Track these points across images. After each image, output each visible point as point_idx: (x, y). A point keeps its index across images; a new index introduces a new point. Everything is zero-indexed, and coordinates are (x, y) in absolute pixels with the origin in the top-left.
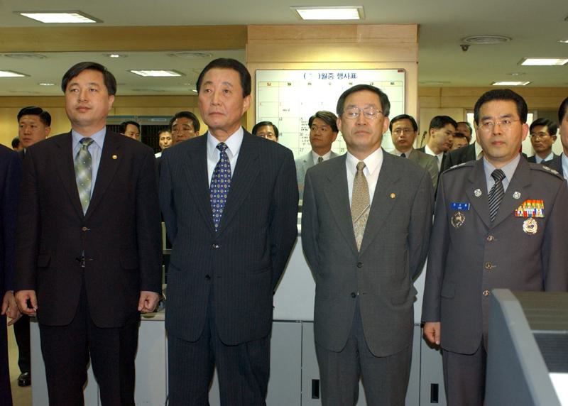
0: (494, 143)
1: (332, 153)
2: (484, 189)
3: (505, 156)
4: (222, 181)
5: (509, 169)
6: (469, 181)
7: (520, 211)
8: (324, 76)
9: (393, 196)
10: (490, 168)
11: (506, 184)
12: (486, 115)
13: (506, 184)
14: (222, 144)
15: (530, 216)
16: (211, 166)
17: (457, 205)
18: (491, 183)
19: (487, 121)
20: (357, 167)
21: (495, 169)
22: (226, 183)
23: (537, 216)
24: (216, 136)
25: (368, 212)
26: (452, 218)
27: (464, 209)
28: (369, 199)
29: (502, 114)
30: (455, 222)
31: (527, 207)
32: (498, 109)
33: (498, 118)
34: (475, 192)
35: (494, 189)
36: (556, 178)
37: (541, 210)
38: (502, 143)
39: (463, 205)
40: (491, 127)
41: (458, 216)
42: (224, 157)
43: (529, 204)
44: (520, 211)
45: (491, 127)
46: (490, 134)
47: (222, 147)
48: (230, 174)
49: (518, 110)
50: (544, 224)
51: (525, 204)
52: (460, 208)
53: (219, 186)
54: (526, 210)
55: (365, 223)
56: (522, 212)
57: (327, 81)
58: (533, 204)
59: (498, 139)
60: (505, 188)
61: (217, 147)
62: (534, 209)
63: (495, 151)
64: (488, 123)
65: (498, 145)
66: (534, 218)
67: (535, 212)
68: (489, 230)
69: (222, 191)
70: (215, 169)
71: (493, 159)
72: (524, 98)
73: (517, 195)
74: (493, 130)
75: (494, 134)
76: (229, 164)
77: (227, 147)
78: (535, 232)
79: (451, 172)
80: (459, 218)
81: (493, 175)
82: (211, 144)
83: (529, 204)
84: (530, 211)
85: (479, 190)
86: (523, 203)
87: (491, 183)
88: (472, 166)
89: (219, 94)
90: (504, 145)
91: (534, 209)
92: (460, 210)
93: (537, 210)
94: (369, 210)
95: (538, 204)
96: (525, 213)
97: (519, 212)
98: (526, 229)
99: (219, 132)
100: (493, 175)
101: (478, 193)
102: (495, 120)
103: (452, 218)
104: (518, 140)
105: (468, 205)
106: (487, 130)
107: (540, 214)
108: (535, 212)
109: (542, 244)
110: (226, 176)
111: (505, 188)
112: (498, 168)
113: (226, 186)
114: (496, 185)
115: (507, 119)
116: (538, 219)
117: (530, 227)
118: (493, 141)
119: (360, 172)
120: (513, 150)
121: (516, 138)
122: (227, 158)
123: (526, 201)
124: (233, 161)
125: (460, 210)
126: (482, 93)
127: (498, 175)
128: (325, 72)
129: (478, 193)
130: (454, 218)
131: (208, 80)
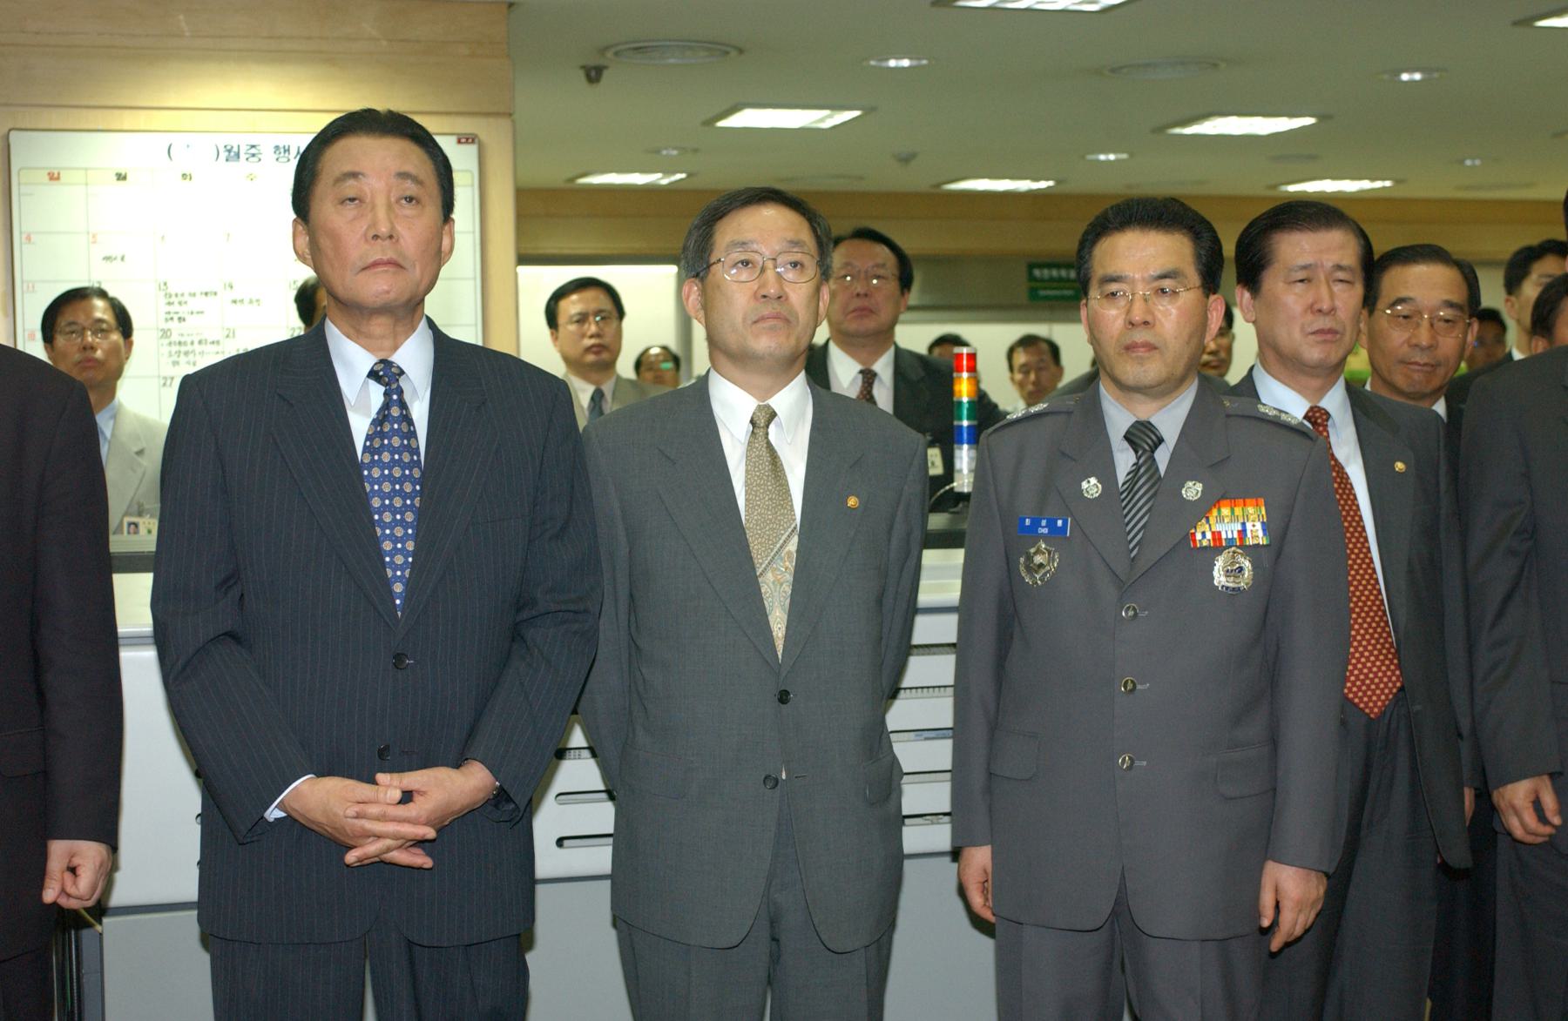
0: (1130, 348)
1: (619, 378)
2: (1106, 472)
3: (1159, 385)
4: (397, 472)
5: (1170, 419)
6: (1063, 454)
7: (1203, 534)
8: (233, 155)
9: (852, 502)
10: (1118, 417)
11: (1162, 457)
12: (1112, 270)
13: (1162, 457)
14: (386, 363)
15: (1230, 541)
16: (360, 426)
17: (1036, 523)
19: (1114, 287)
20: (752, 422)
21: (1134, 420)
22: (410, 478)
23: (1250, 541)
24: (357, 335)
25: (793, 546)
26: (1022, 560)
28: (792, 509)
29: (1158, 273)
30: (1032, 569)
31: (1221, 519)
32: (1139, 254)
33: (1143, 279)
34: (1190, 484)
35: (1135, 473)
36: (1297, 438)
37: (1259, 526)
38: (1151, 347)
39: (1051, 524)
40: (1122, 303)
41: (1038, 552)
42: (395, 400)
43: (1226, 511)
44: (1203, 534)
45: (1122, 303)
46: (1119, 323)
47: (386, 374)
48: (417, 451)
49: (1198, 257)
50: (1270, 559)
51: (1215, 512)
52: (1045, 531)
53: (387, 487)
55: (789, 577)
56: (1209, 535)
57: (242, 166)
58: (1238, 511)
59: (1140, 336)
60: (1162, 468)
61: (373, 374)
62: (1241, 523)
63: (1131, 371)
64: (1113, 294)
65: (1141, 352)
66: (1242, 546)
67: (1242, 533)
68: (1125, 589)
69: (398, 502)
70: (369, 437)
71: (1124, 388)
72: (1216, 226)
74: (1128, 312)
75: (1131, 324)
76: (410, 422)
77: (402, 372)
79: (1006, 431)
80: (1038, 559)
81: (1128, 437)
82: (348, 364)
83: (1226, 511)
84: (1229, 530)
85: (1093, 480)
86: (1210, 511)
88: (1069, 413)
89: (389, 207)
90: (1156, 354)
91: (1241, 523)
93: (1249, 526)
94: (795, 539)
95: (1251, 510)
96: (1217, 536)
97: (1199, 536)
99: (379, 325)
100: (1128, 437)
101: (1091, 487)
102: (1133, 282)
103: (1022, 560)
104: (1195, 341)
105: (1065, 523)
106: (1113, 312)
108: (1242, 533)
109: (1266, 613)
110: (406, 458)
111: (1162, 468)
112: (1143, 417)
113: (408, 488)
114: (1137, 466)
115: (1167, 284)
116: (1252, 551)
118: (1128, 342)
119: (760, 432)
120: (1180, 370)
121: (1190, 337)
122: (403, 405)
123: (1217, 503)
124: (420, 411)
125: (1043, 536)
126: (1095, 212)
127: (1143, 437)
128: (233, 141)
129: (1091, 487)
130: (1029, 558)
131: (348, 168)
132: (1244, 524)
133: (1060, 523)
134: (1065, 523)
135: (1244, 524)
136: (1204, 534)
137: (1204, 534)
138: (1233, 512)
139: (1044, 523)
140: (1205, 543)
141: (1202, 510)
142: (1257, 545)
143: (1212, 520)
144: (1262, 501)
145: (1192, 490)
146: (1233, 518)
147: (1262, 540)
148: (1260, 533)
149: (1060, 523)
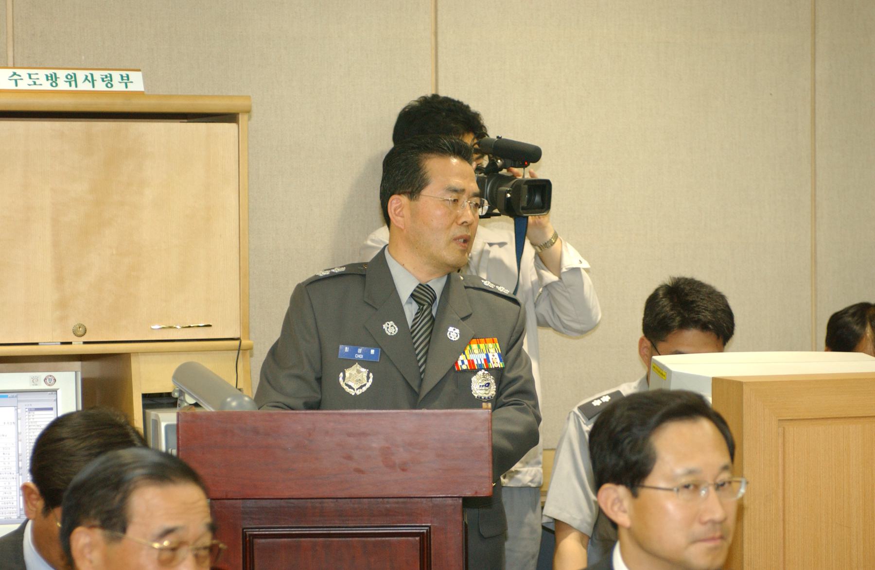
2: (400, 319)
7: (463, 362)
15: (481, 365)
37: (497, 356)
43: (474, 346)
52: (361, 357)
58: (482, 346)
66: (488, 369)
67: (487, 360)
86: (465, 348)
92: (363, 363)
93: (490, 355)
95: (490, 345)
96: (471, 362)
97: (460, 363)
101: (391, 328)
107: (496, 362)
108: (487, 360)
129: (391, 328)
132: (487, 355)
135: (487, 355)
136: (463, 362)
137: (463, 362)
138: (479, 347)
140: (464, 367)
141: (460, 347)
142: (497, 369)
144: (495, 339)
146: (481, 351)
147: (500, 365)
148: (498, 360)
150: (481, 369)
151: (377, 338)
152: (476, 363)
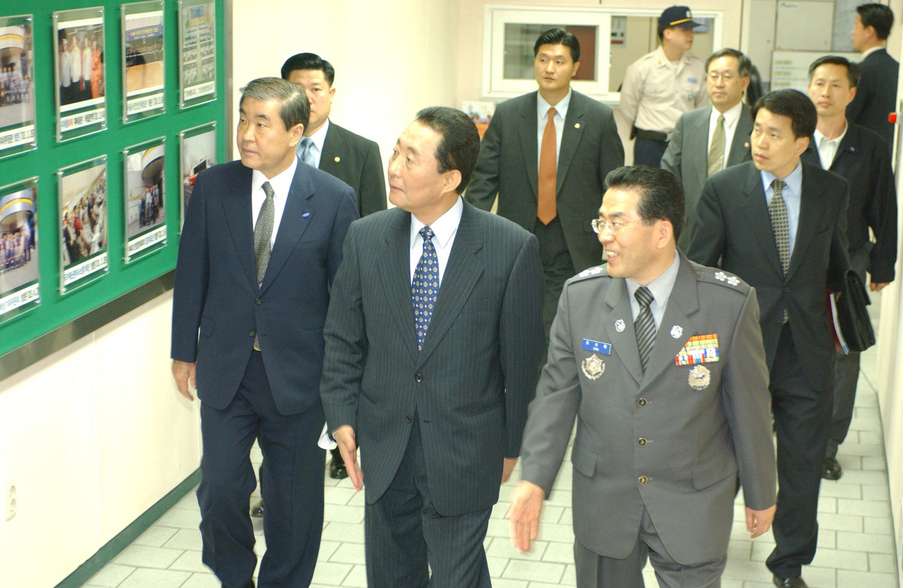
7: (683, 357)
18: (636, 310)
23: (708, 360)
27: (602, 354)
39: (600, 346)
44: (683, 357)
51: (689, 343)
52: (597, 349)
54: (690, 353)
58: (702, 342)
66: (704, 364)
67: (704, 356)
73: (677, 332)
78: (708, 384)
83: (695, 343)
84: (697, 355)
87: (636, 310)
91: (704, 349)
93: (708, 351)
96: (690, 358)
98: (693, 383)
108: (704, 356)
117: (701, 378)
125: (596, 352)
133: (605, 347)
134: (608, 346)
139: (596, 345)
140: (684, 363)
141: (682, 343)
142: (712, 363)
143: (688, 348)
145: (677, 332)
147: (716, 359)
149: (605, 347)
150: (696, 365)
151: (607, 333)
152: (694, 358)
